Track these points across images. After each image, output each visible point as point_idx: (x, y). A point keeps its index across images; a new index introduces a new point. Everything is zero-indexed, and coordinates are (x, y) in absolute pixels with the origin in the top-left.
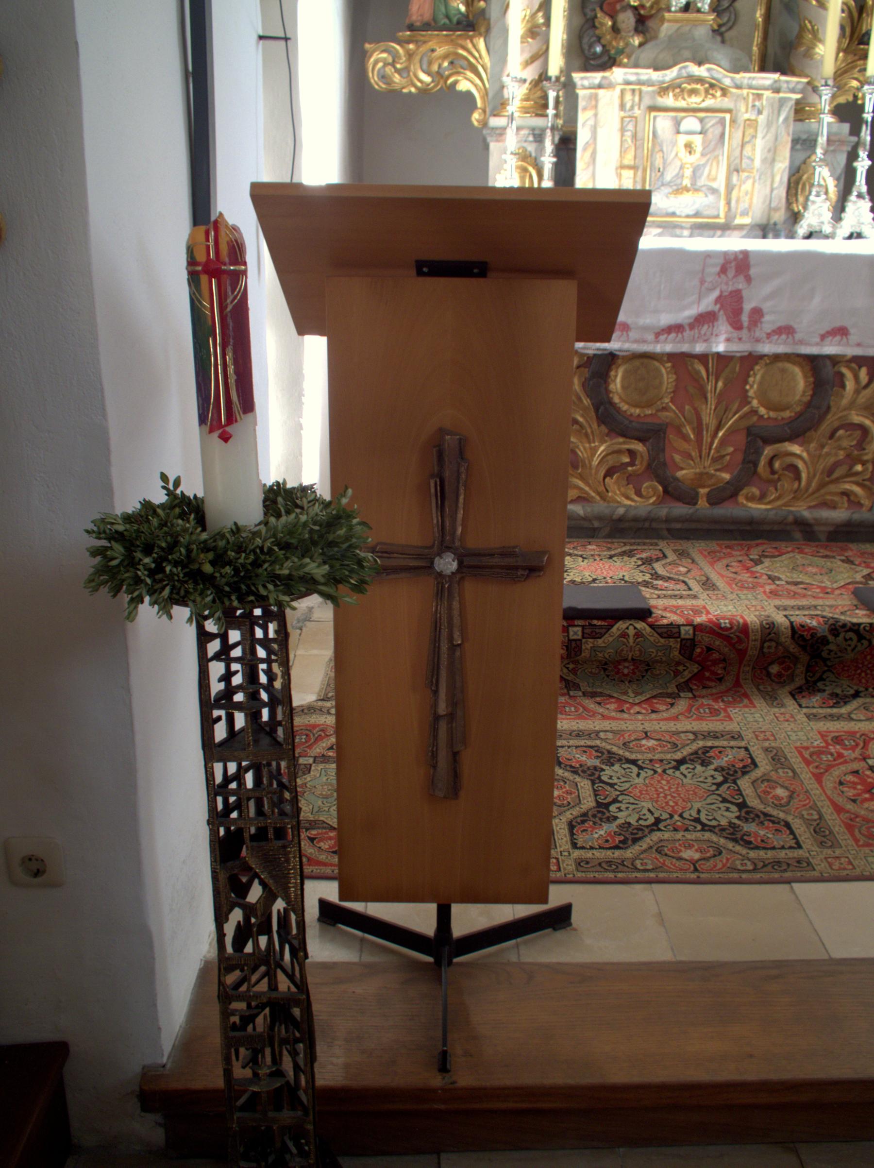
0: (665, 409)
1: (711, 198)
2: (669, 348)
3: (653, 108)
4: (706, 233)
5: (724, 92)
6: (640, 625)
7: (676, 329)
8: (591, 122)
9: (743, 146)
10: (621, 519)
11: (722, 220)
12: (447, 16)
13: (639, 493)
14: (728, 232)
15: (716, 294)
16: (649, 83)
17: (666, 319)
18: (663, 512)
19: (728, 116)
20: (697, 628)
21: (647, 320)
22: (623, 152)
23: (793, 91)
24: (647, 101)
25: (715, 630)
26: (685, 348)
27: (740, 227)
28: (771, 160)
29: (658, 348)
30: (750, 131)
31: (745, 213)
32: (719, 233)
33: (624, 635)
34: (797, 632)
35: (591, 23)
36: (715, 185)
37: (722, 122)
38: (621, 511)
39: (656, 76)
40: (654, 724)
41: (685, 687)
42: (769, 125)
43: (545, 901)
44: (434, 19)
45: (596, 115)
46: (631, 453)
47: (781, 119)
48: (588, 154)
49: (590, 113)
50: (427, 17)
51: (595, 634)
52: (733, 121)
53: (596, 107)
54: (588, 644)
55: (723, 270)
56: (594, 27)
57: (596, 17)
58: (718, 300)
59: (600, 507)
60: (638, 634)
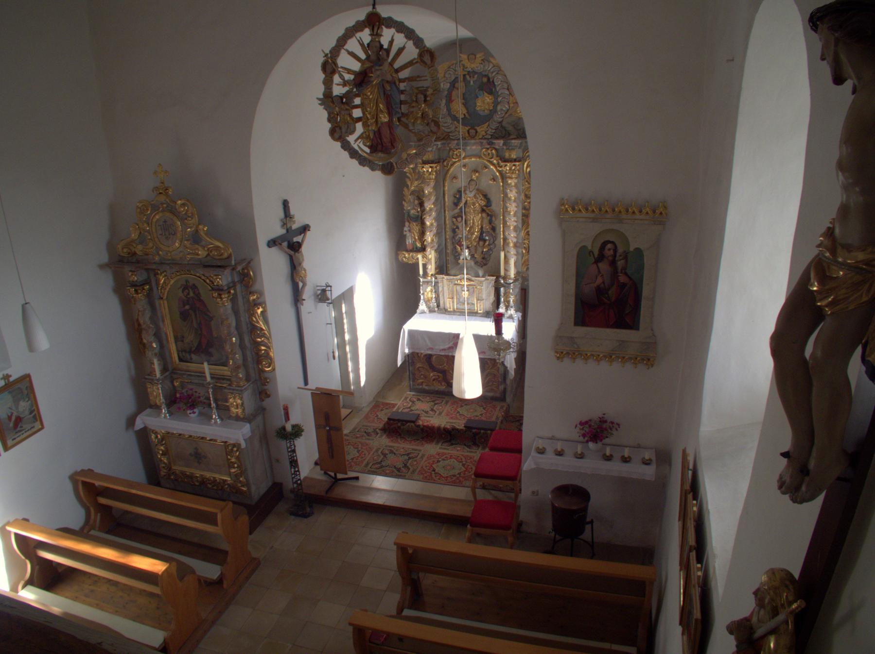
0: (445, 366)
1: (472, 306)
2: (443, 354)
3: (455, 284)
4: (472, 315)
5: (473, 281)
6: (413, 424)
7: (444, 350)
8: (442, 286)
9: (479, 294)
10: (437, 391)
11: (476, 311)
12: (417, 248)
13: (441, 384)
14: (477, 315)
15: (452, 343)
16: (453, 279)
17: (442, 347)
18: (447, 390)
19: (475, 287)
20: (424, 426)
21: (437, 347)
22: (449, 295)
23: (493, 280)
24: (454, 283)
25: (427, 427)
26: (447, 354)
27: (480, 313)
28: (488, 295)
29: (441, 354)
30: (480, 291)
31: (480, 310)
32: (474, 315)
33: (409, 426)
34: (445, 429)
35: (455, 248)
36: (473, 302)
37: (473, 288)
38: (437, 389)
39: (454, 277)
40: (402, 445)
41: (423, 438)
42: (488, 287)
43: (346, 474)
44: (413, 249)
45: (443, 285)
46: (439, 376)
47: (490, 286)
48: (442, 293)
49: (441, 284)
50: (411, 248)
51: (403, 425)
52: (476, 288)
53: (443, 282)
54: (402, 427)
55: (454, 337)
56: (456, 249)
57: (456, 247)
58: (453, 344)
59: (432, 388)
60: (412, 426)
